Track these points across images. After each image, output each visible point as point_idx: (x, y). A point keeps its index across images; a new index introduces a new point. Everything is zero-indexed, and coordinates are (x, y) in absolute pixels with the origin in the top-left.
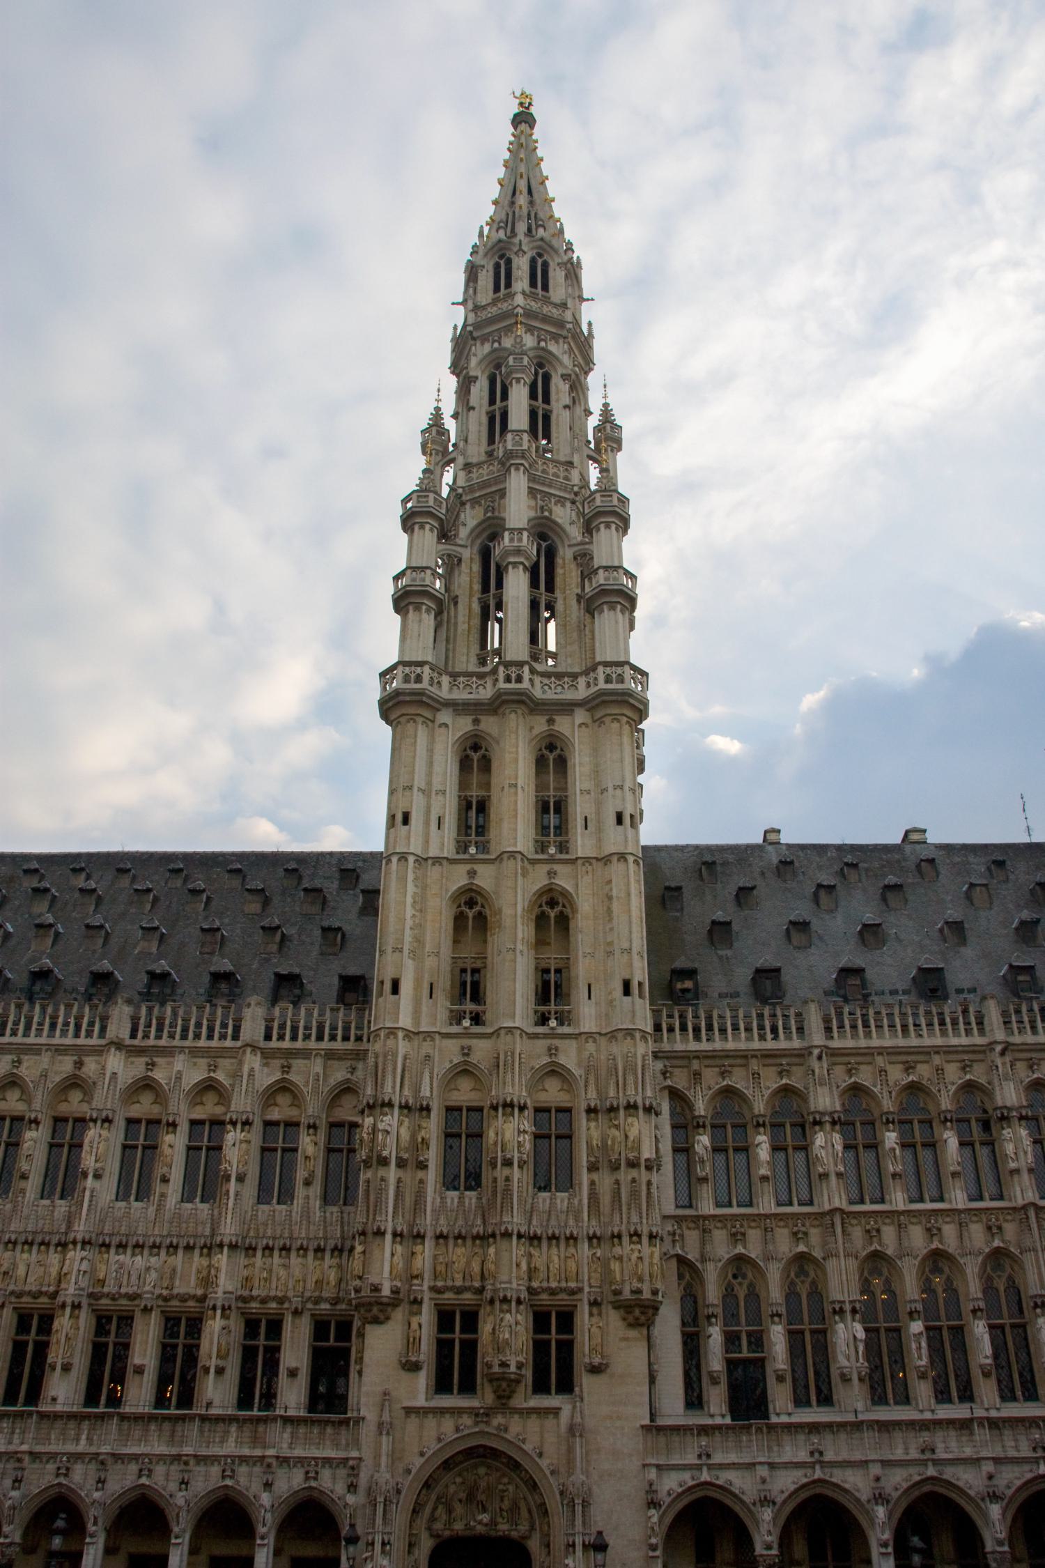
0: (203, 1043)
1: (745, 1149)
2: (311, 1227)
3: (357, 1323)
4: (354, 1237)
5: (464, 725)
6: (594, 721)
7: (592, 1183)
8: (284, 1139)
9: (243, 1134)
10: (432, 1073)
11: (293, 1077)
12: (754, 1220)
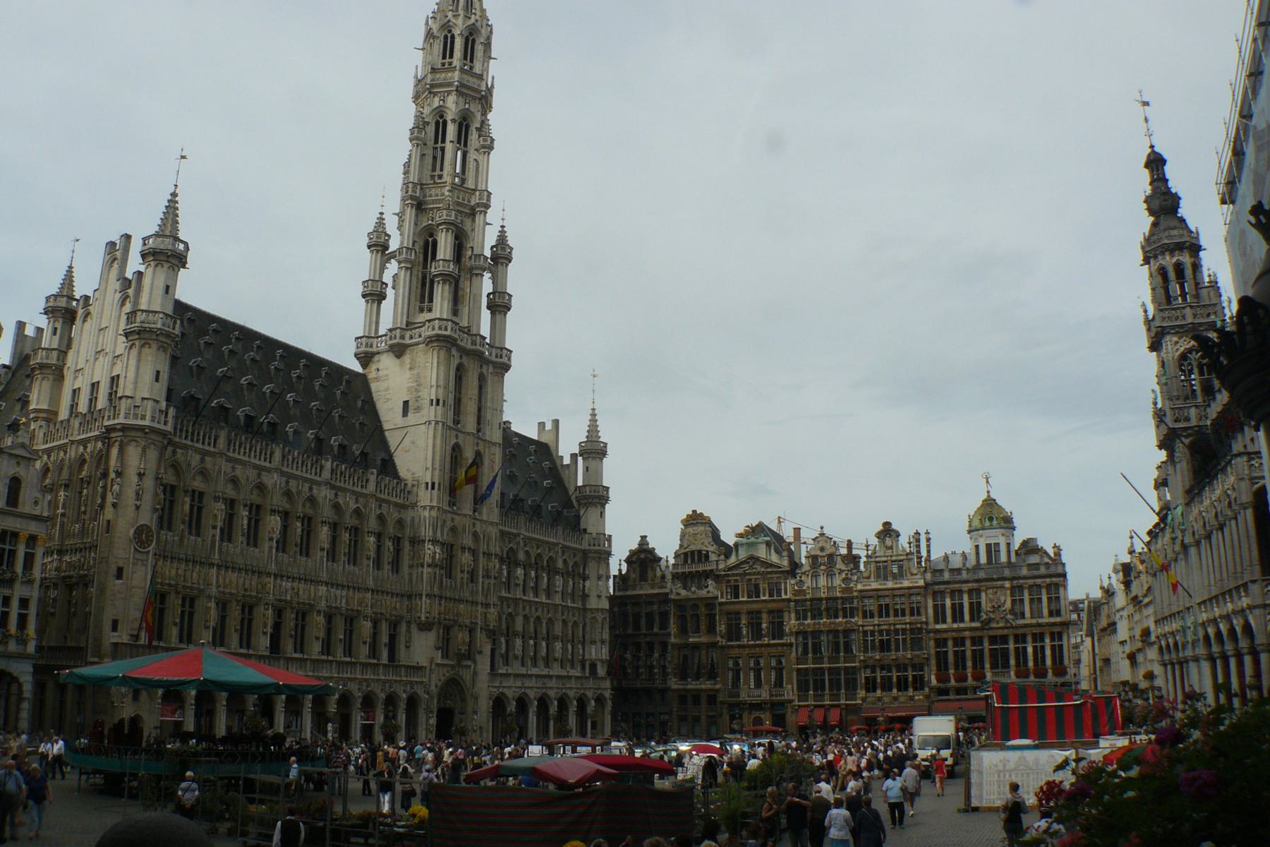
0: (356, 489)
3: (403, 627)
7: (483, 583)
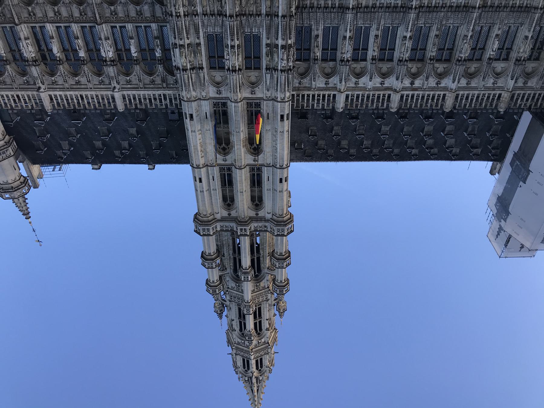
0: (361, 93)
1: (141, 50)
2: (315, 17)
4: (295, 14)
5: (261, 213)
6: (213, 214)
7: (198, 38)
8: (328, 53)
9: (344, 56)
10: (266, 84)
11: (324, 80)
12: (134, 20)
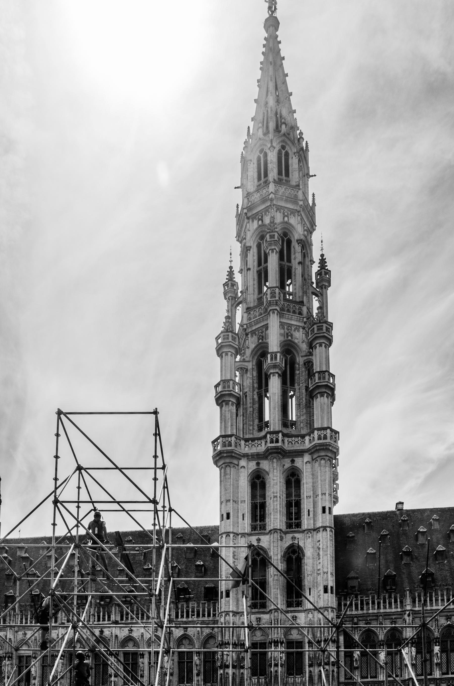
5: (252, 465)
8: (187, 657)
